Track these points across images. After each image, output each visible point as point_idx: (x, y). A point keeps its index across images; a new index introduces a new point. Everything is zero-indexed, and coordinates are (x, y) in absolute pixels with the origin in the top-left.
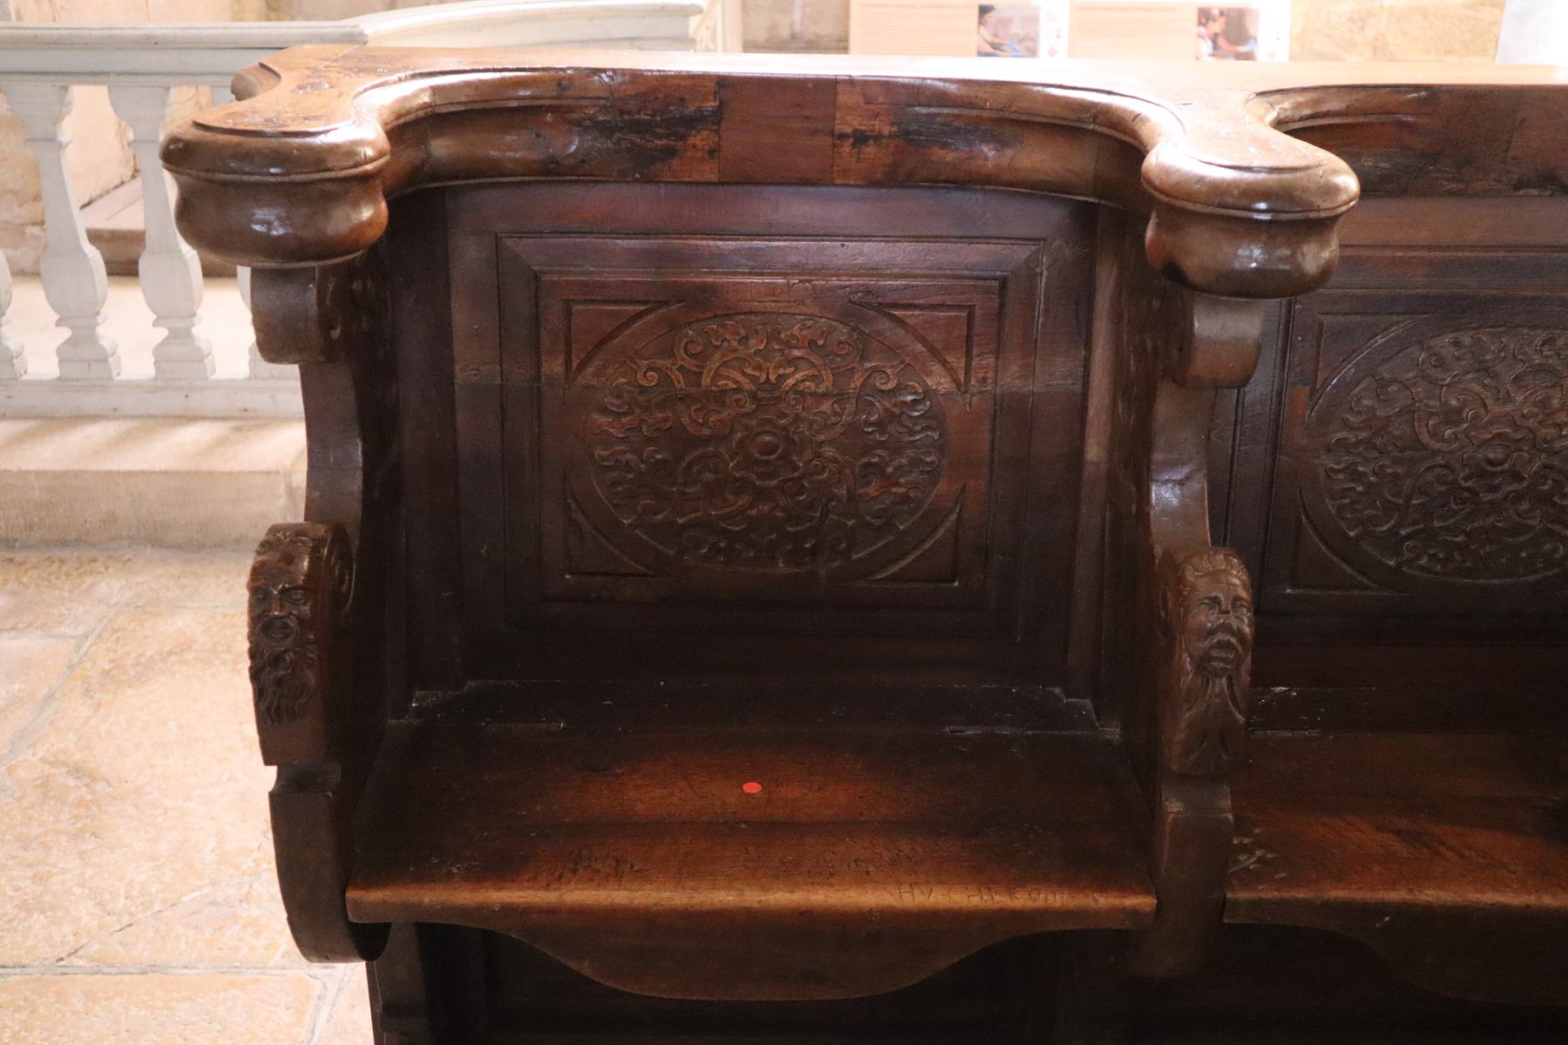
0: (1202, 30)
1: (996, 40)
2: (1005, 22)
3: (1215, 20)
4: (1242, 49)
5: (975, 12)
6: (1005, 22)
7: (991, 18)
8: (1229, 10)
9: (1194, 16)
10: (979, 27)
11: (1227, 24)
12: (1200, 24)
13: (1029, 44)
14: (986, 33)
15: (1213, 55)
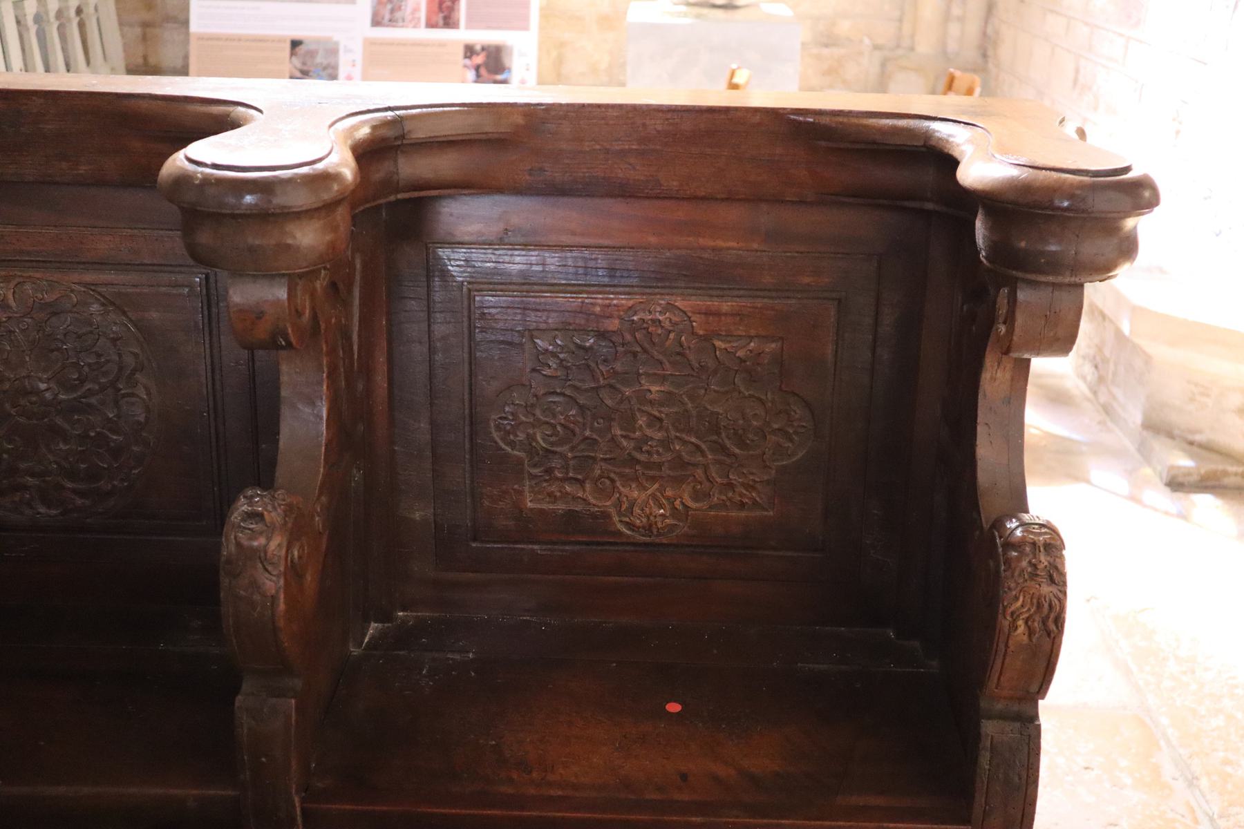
0: (468, 62)
1: (305, 68)
2: (312, 54)
3: (478, 54)
4: (499, 77)
5: (288, 46)
6: (312, 54)
7: (301, 49)
8: (489, 46)
9: (461, 52)
10: (291, 58)
11: (488, 57)
12: (466, 57)
13: (330, 71)
14: (296, 61)
15: (476, 82)
